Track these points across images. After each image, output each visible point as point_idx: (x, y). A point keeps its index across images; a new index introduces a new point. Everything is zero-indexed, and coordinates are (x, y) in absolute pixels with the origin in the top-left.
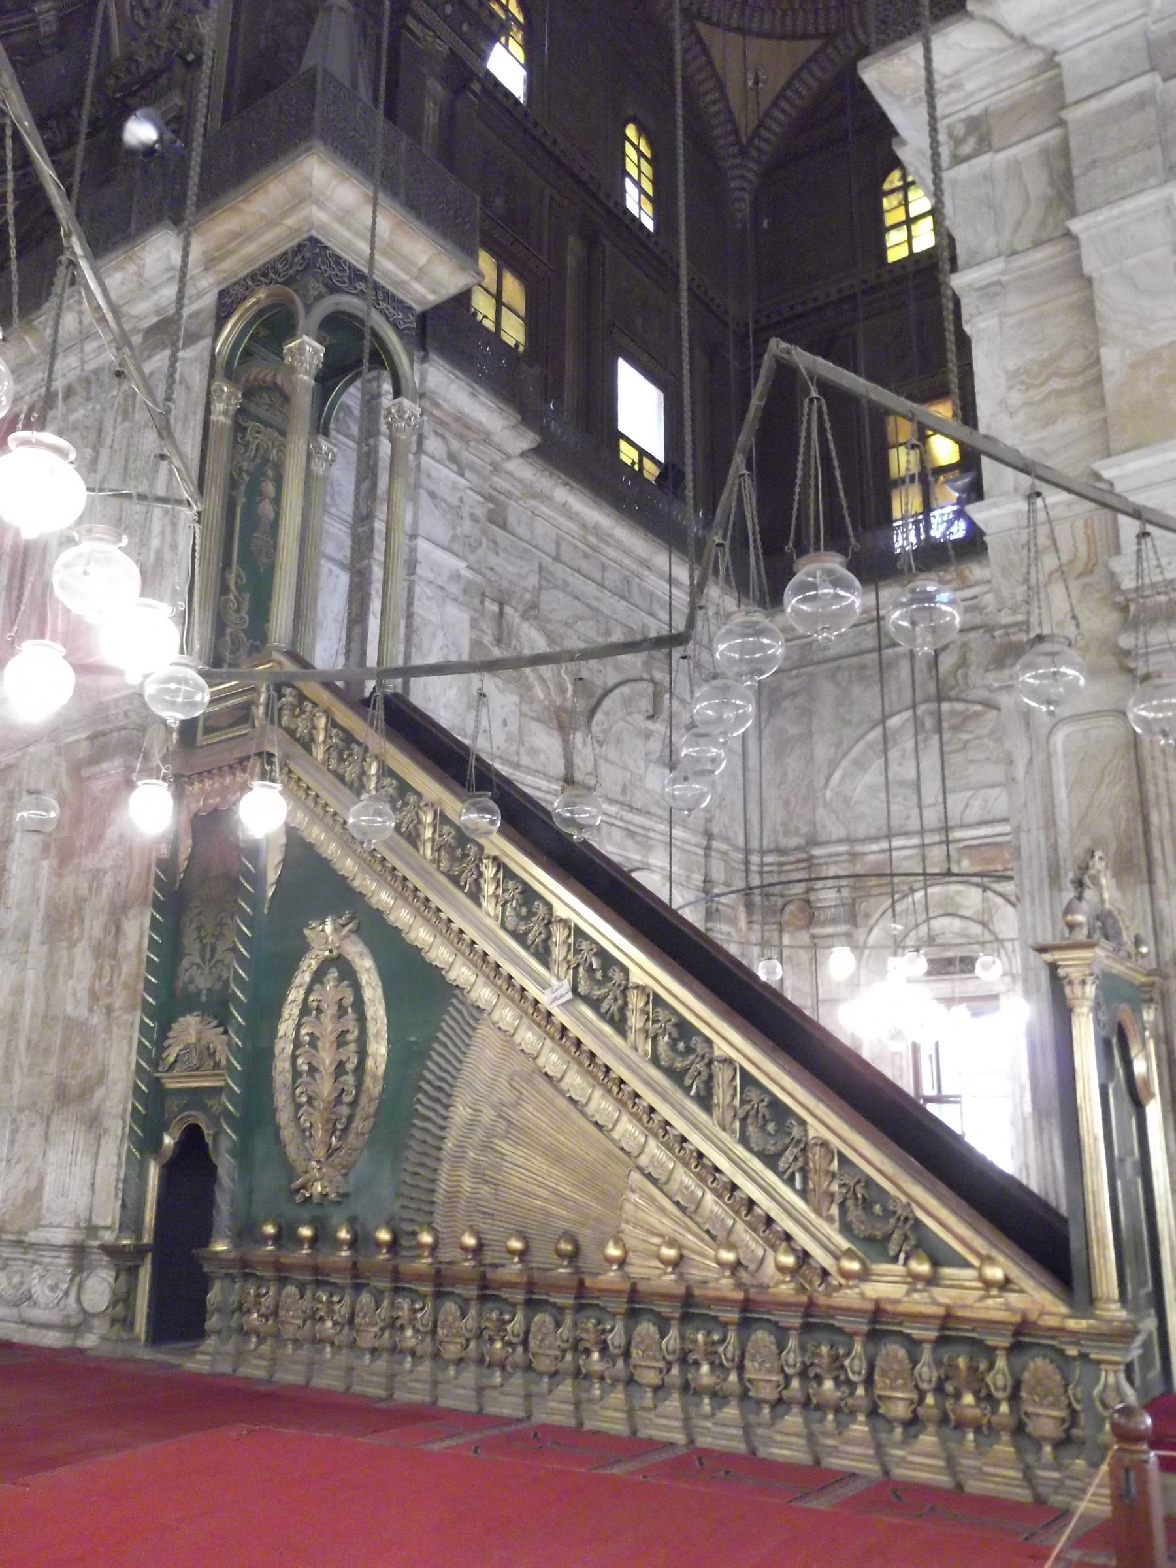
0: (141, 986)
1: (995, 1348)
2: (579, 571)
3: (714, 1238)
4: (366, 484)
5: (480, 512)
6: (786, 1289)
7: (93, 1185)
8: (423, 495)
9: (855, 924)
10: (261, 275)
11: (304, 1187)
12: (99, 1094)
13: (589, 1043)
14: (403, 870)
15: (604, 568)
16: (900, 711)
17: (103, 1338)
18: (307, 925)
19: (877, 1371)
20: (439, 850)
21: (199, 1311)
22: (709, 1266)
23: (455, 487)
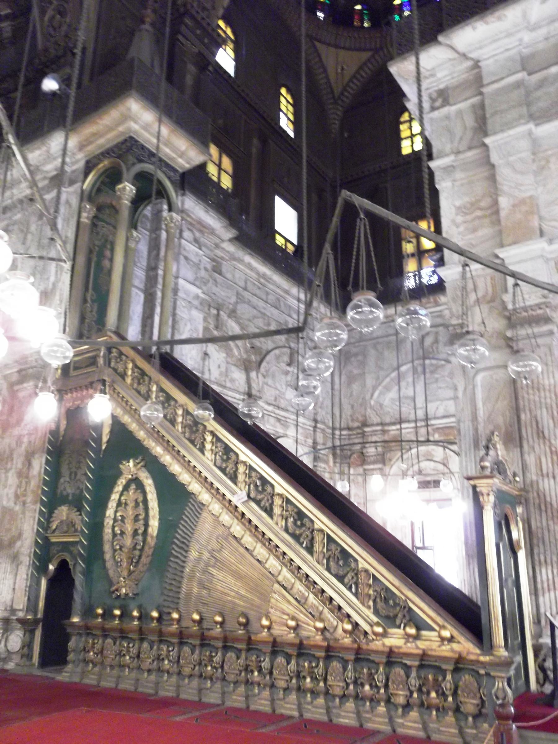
0: (40, 492)
1: (446, 670)
2: (256, 295)
3: (313, 616)
4: (155, 252)
5: (209, 267)
6: (347, 641)
7: (14, 589)
8: (182, 258)
9: (384, 463)
10: (106, 153)
11: (117, 590)
12: (18, 544)
13: (255, 521)
14: (168, 437)
15: (267, 294)
16: (406, 364)
17: (17, 665)
18: (121, 463)
19: (390, 681)
20: (185, 427)
21: (66, 652)
22: (311, 630)
23: (197, 255)
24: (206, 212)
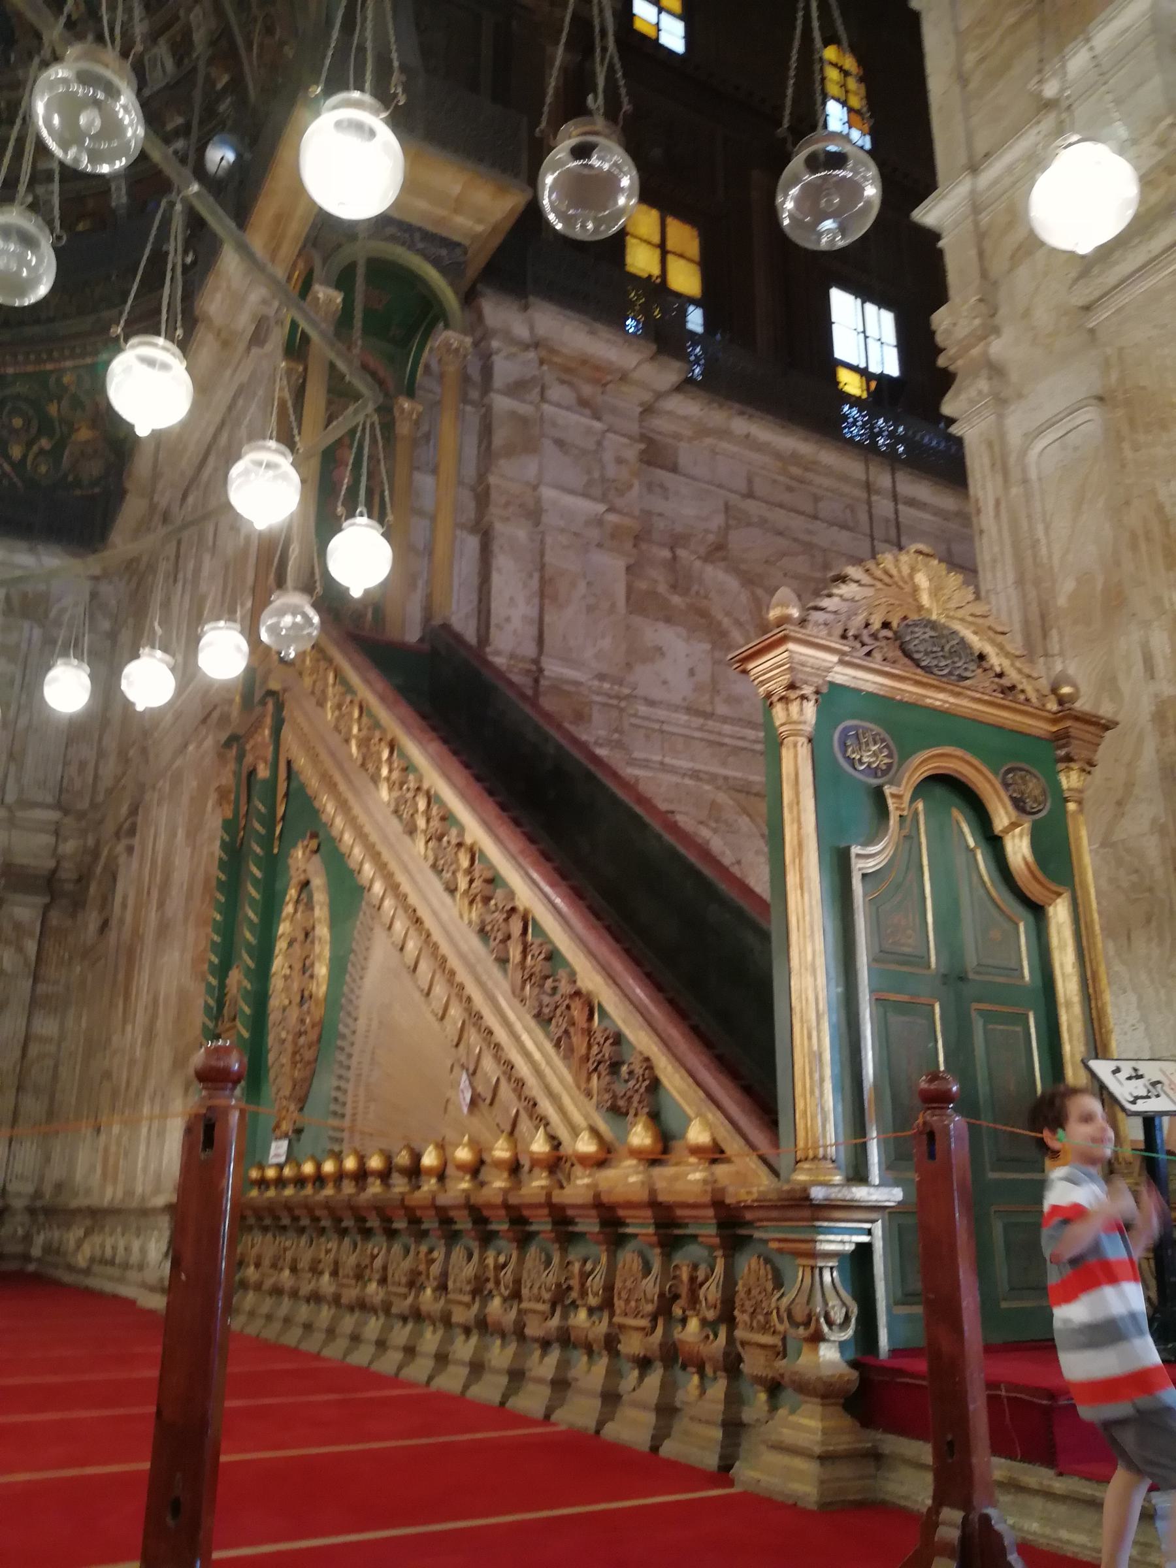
5: (632, 453)
15: (817, 499)
23: (589, 431)
24: (592, 332)
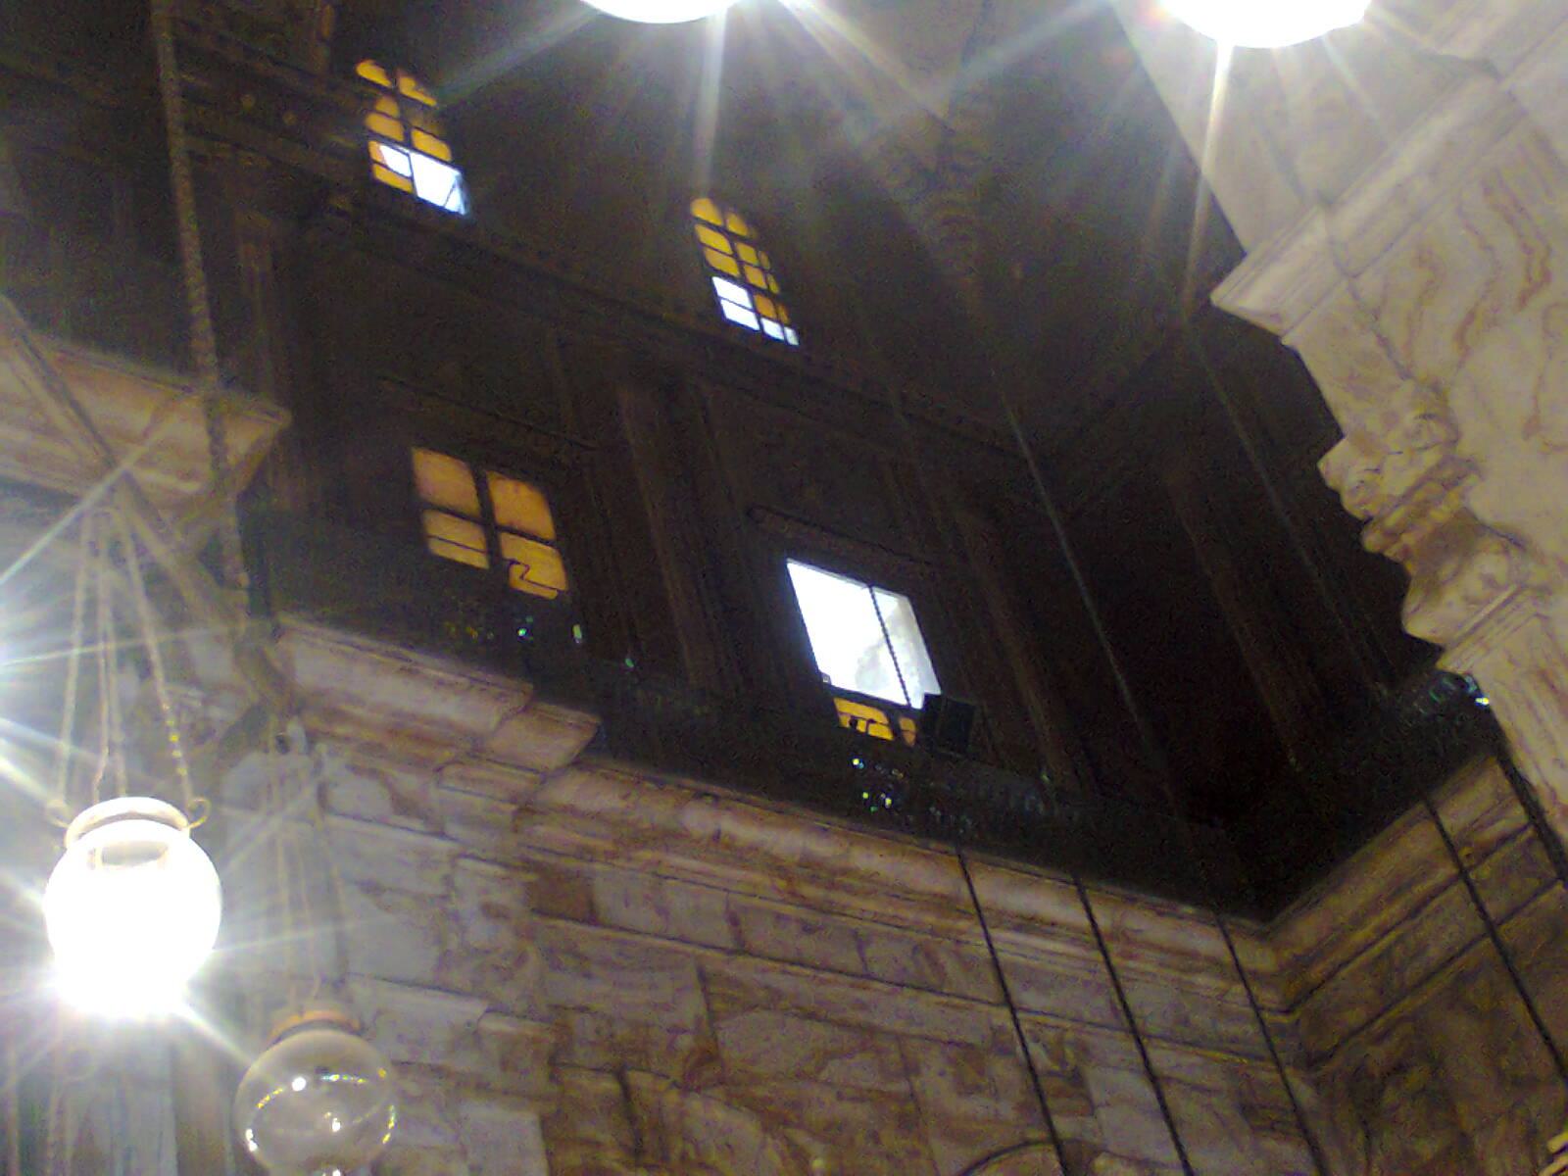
23: (426, 860)
